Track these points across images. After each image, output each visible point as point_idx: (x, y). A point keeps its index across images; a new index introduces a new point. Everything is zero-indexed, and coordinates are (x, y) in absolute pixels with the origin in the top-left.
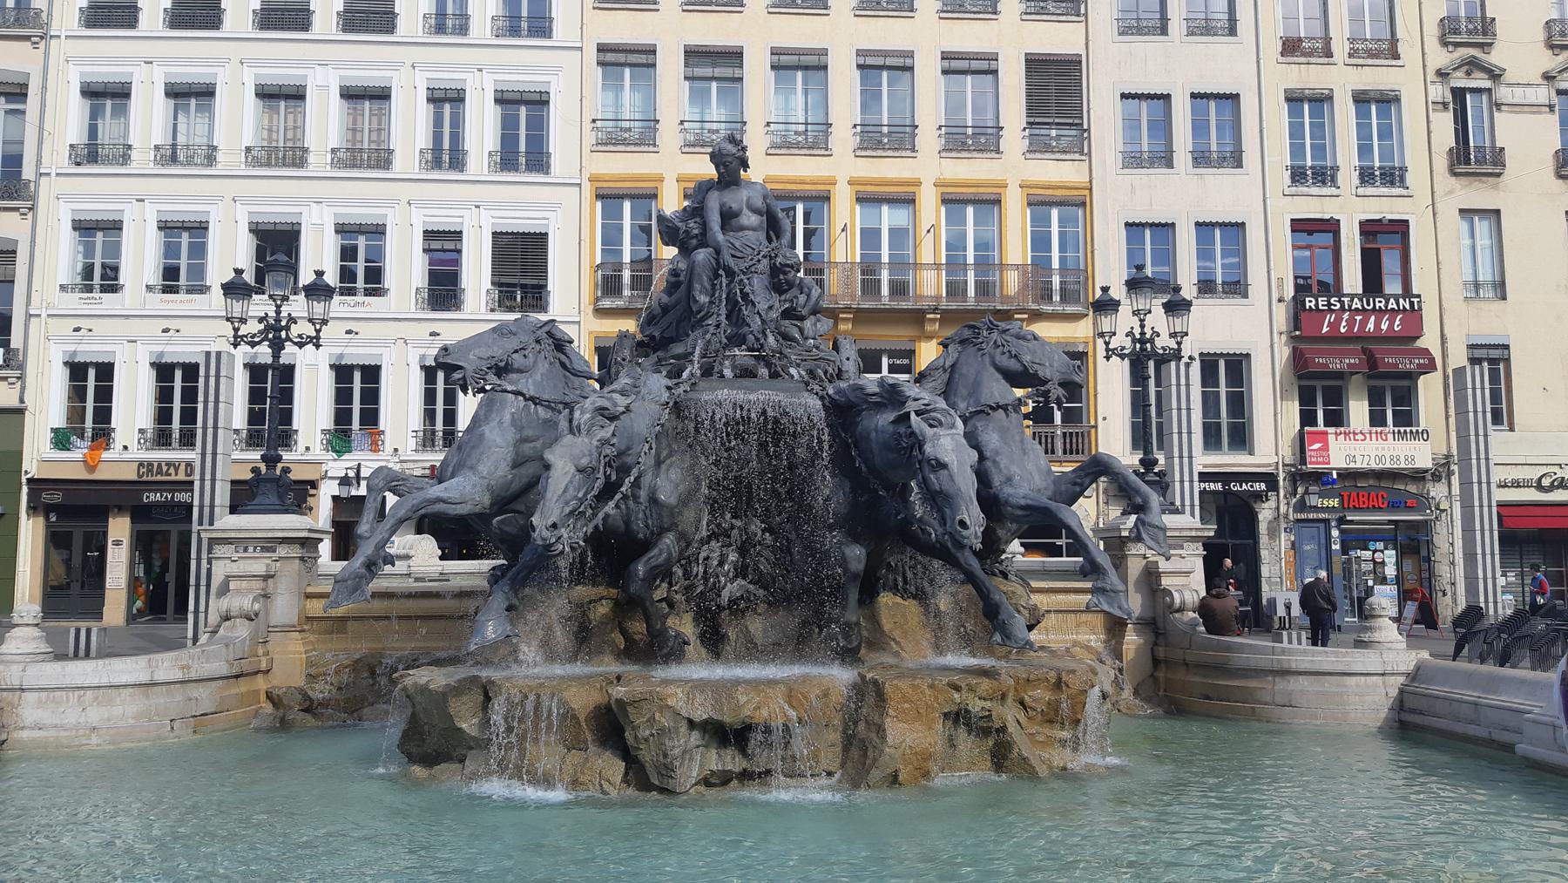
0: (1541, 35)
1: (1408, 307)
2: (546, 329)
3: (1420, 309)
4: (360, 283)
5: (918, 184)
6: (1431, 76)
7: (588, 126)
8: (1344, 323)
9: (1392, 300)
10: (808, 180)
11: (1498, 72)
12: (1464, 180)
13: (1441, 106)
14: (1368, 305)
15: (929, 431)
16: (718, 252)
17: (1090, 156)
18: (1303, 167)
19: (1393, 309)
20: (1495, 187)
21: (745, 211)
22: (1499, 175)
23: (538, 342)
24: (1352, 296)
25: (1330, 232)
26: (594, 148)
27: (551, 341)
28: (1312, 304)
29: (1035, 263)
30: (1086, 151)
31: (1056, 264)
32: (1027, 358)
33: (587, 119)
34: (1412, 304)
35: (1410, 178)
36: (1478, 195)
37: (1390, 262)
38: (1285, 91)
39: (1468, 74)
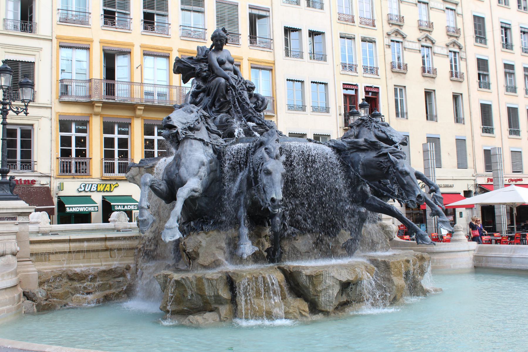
0: (416, 25)
6: (385, 35)
7: (55, 12)
11: (405, 36)
12: (395, 74)
13: (388, 46)
15: (398, 161)
17: (274, 51)
18: (346, 64)
20: (404, 78)
21: (227, 62)
22: (405, 74)
25: (353, 89)
30: (272, 48)
32: (388, 133)
33: (55, 9)
36: (399, 81)
38: (340, 34)
39: (396, 35)
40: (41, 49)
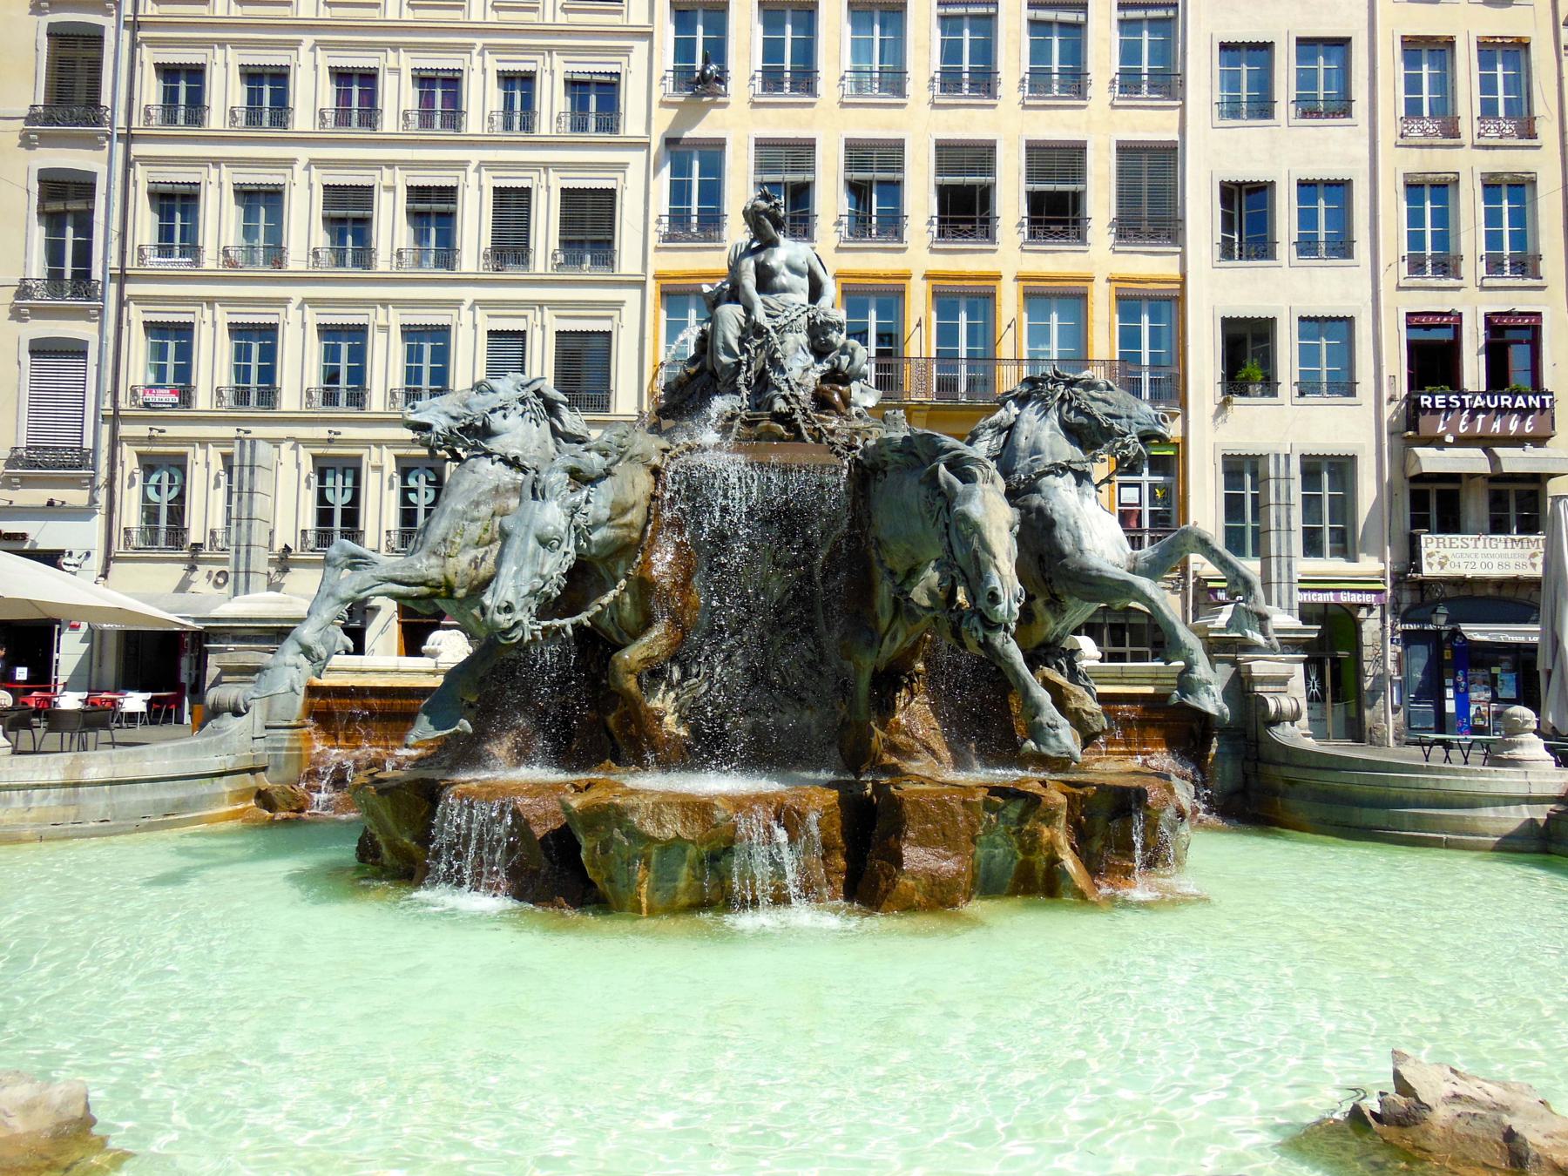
1: (1538, 405)
2: (536, 386)
3: (1552, 407)
4: (426, 383)
5: (998, 277)
8: (1463, 423)
9: (1520, 398)
10: (882, 274)
14: (1493, 403)
16: (749, 310)
19: (1520, 408)
23: (523, 401)
24: (1474, 394)
26: (662, 245)
27: (539, 401)
28: (1428, 404)
29: (1124, 358)
31: (1146, 360)
34: (1543, 402)
35: (1544, 267)
37: (1518, 357)
40: (622, 303)
